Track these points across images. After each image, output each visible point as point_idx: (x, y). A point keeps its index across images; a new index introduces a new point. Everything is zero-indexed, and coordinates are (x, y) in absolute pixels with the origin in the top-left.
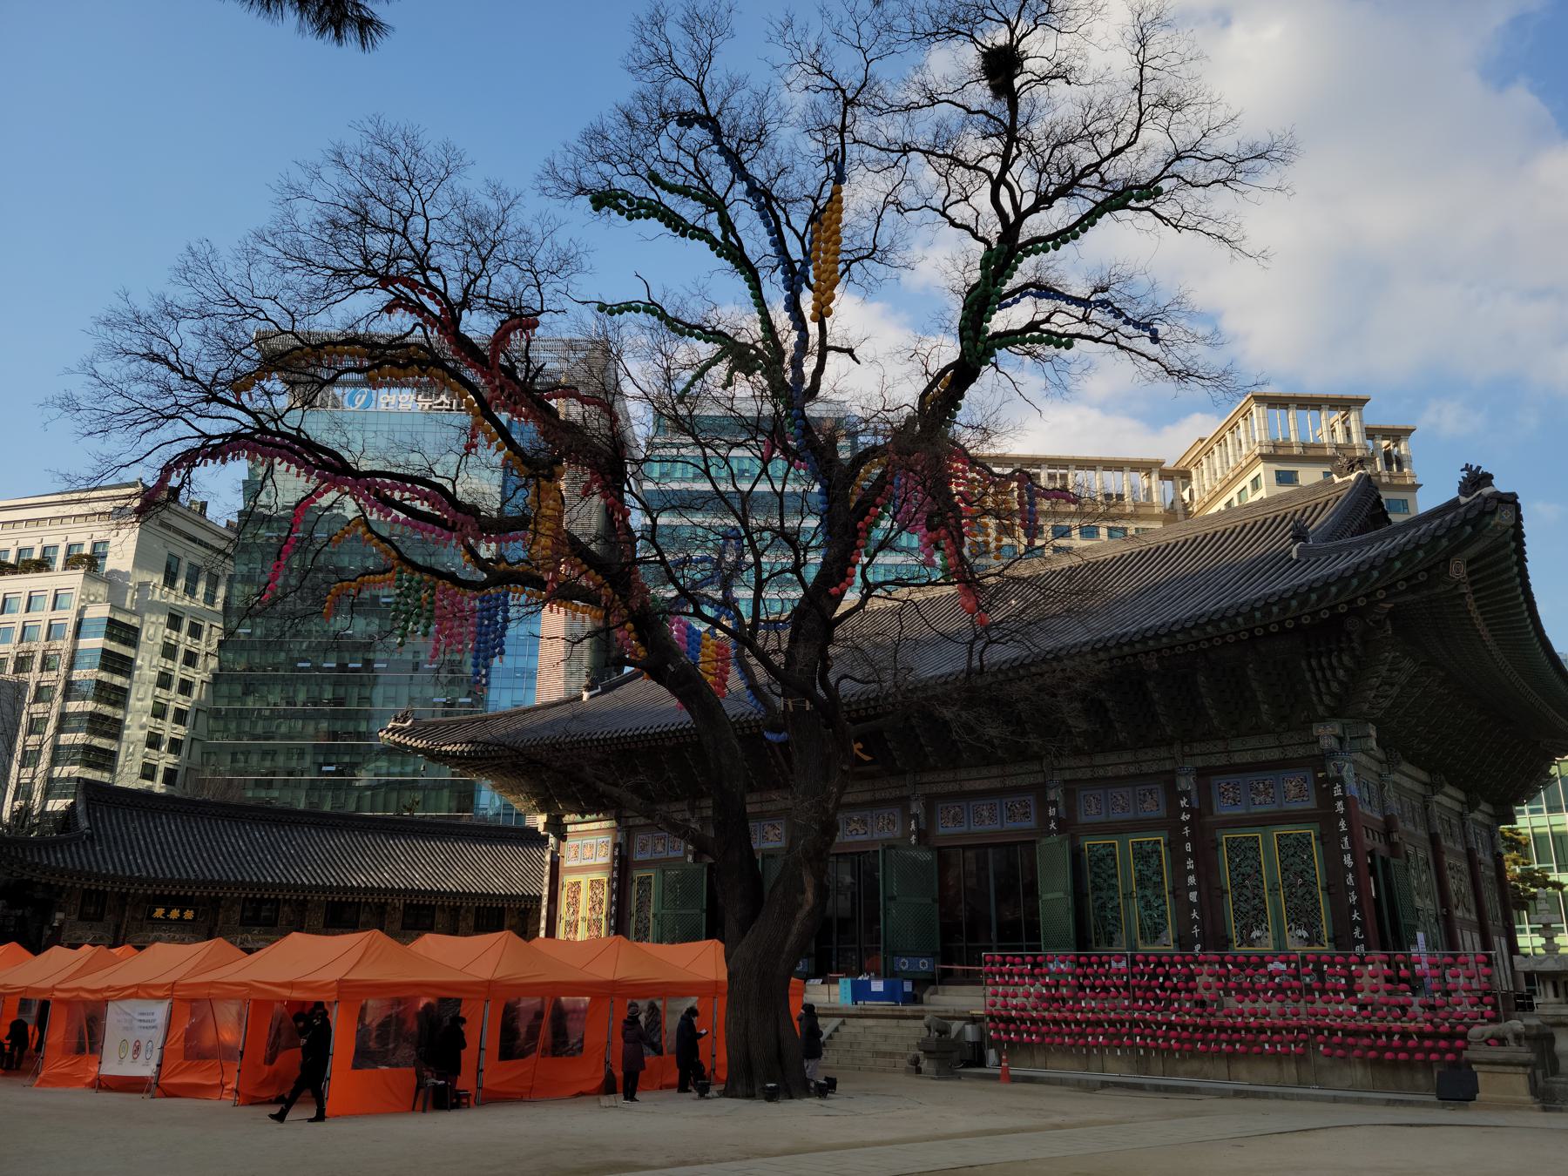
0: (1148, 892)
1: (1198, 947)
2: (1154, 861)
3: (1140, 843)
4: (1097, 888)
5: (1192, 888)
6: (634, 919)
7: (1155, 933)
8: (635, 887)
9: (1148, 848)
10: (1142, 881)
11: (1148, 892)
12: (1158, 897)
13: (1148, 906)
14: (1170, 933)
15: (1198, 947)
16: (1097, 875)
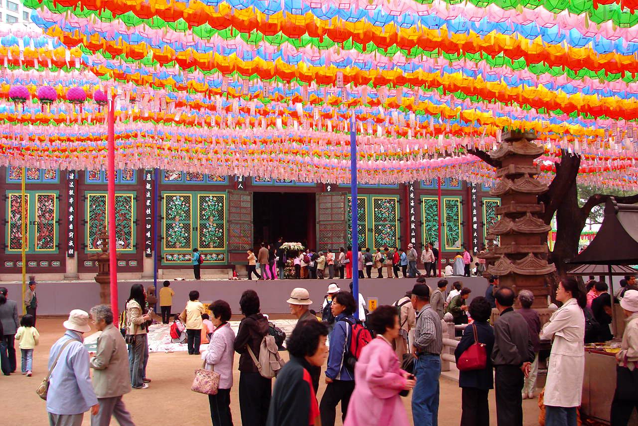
0: (451, 224)
1: (476, 248)
2: (455, 209)
3: (449, 201)
4: (427, 220)
5: (475, 223)
6: (88, 225)
7: (454, 241)
8: (88, 203)
9: (453, 203)
10: (449, 218)
11: (451, 224)
12: (456, 226)
13: (451, 230)
14: (459, 243)
15: (476, 248)
16: (428, 214)
